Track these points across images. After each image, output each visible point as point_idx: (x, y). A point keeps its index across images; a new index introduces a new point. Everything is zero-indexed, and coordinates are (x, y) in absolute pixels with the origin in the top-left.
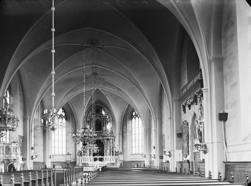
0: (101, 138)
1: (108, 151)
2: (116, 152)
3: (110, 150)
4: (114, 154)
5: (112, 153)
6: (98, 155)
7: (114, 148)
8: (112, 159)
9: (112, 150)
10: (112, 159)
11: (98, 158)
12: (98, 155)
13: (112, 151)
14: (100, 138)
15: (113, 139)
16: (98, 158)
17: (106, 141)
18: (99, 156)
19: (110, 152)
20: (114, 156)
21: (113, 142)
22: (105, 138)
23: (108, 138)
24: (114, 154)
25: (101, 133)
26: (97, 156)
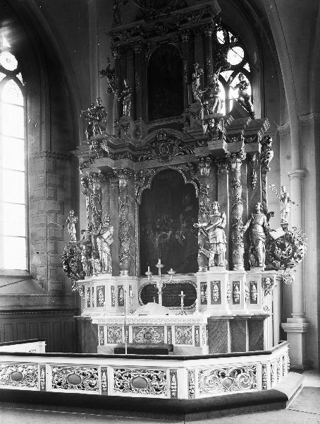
0: (183, 159)
1: (221, 236)
2: (270, 242)
3: (232, 229)
4: (262, 256)
5: (241, 251)
6: (159, 265)
7: (262, 218)
8: (243, 291)
9: (242, 228)
10: (243, 291)
11: (159, 287)
12: (159, 265)
13: (250, 238)
14: (177, 162)
15: (249, 156)
16: (159, 287)
17: (205, 171)
18: (165, 271)
19: (231, 246)
20: (259, 272)
21: (250, 178)
22: (198, 152)
23: (212, 146)
24: (262, 256)
25: (180, 127)
26: (155, 272)
